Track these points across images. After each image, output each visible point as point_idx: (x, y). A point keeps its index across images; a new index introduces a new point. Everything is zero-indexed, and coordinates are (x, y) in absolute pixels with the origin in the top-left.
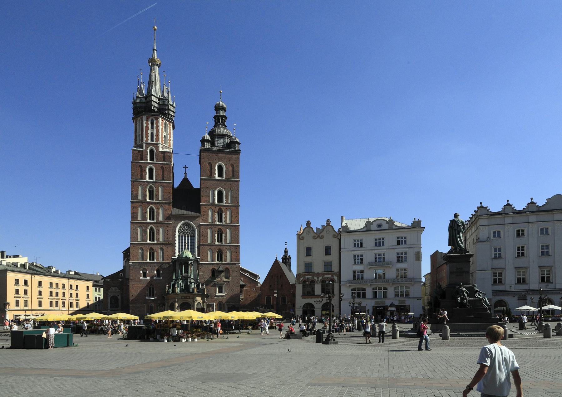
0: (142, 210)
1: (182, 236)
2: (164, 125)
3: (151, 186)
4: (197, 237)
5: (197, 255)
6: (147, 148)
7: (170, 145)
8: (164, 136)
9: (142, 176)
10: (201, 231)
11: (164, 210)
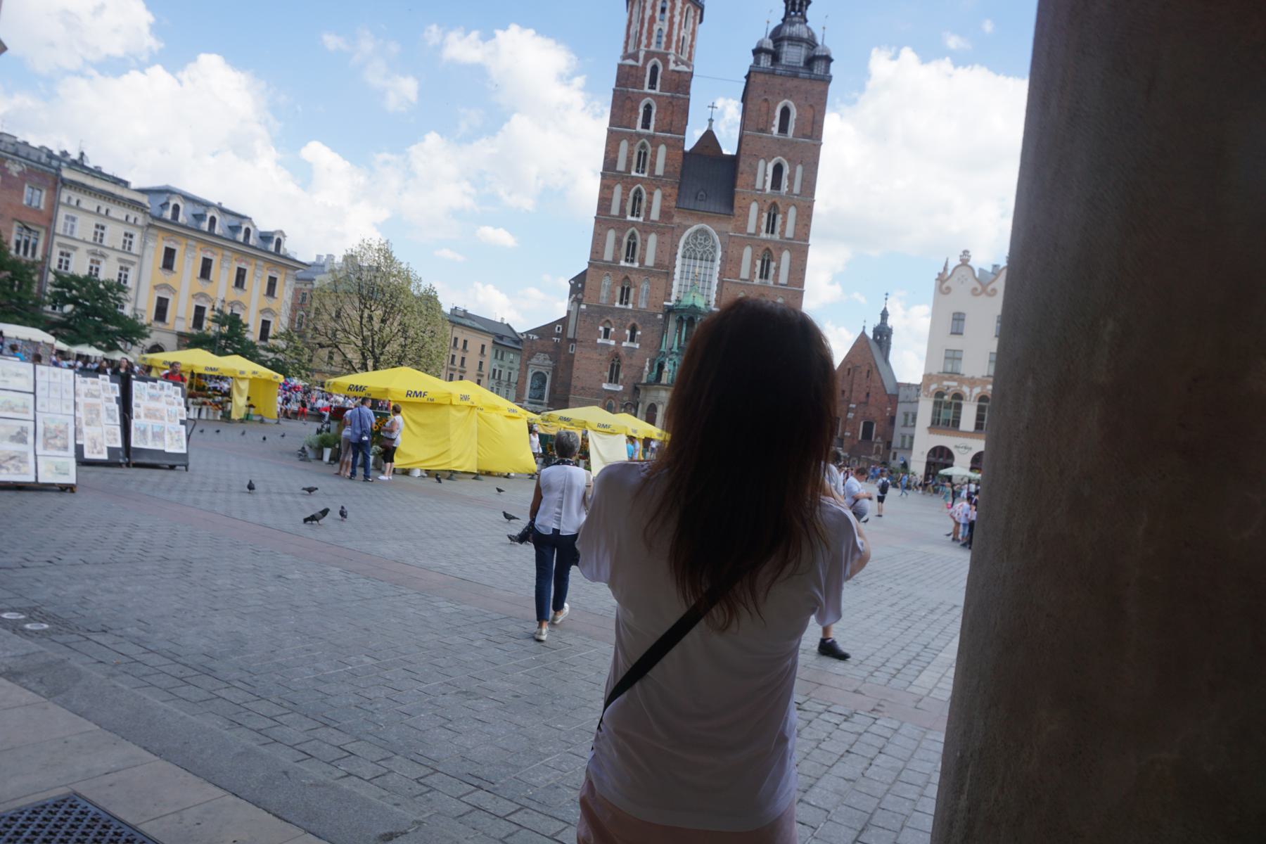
0: (623, 194)
3: (644, 143)
4: (718, 262)
8: (681, 38)
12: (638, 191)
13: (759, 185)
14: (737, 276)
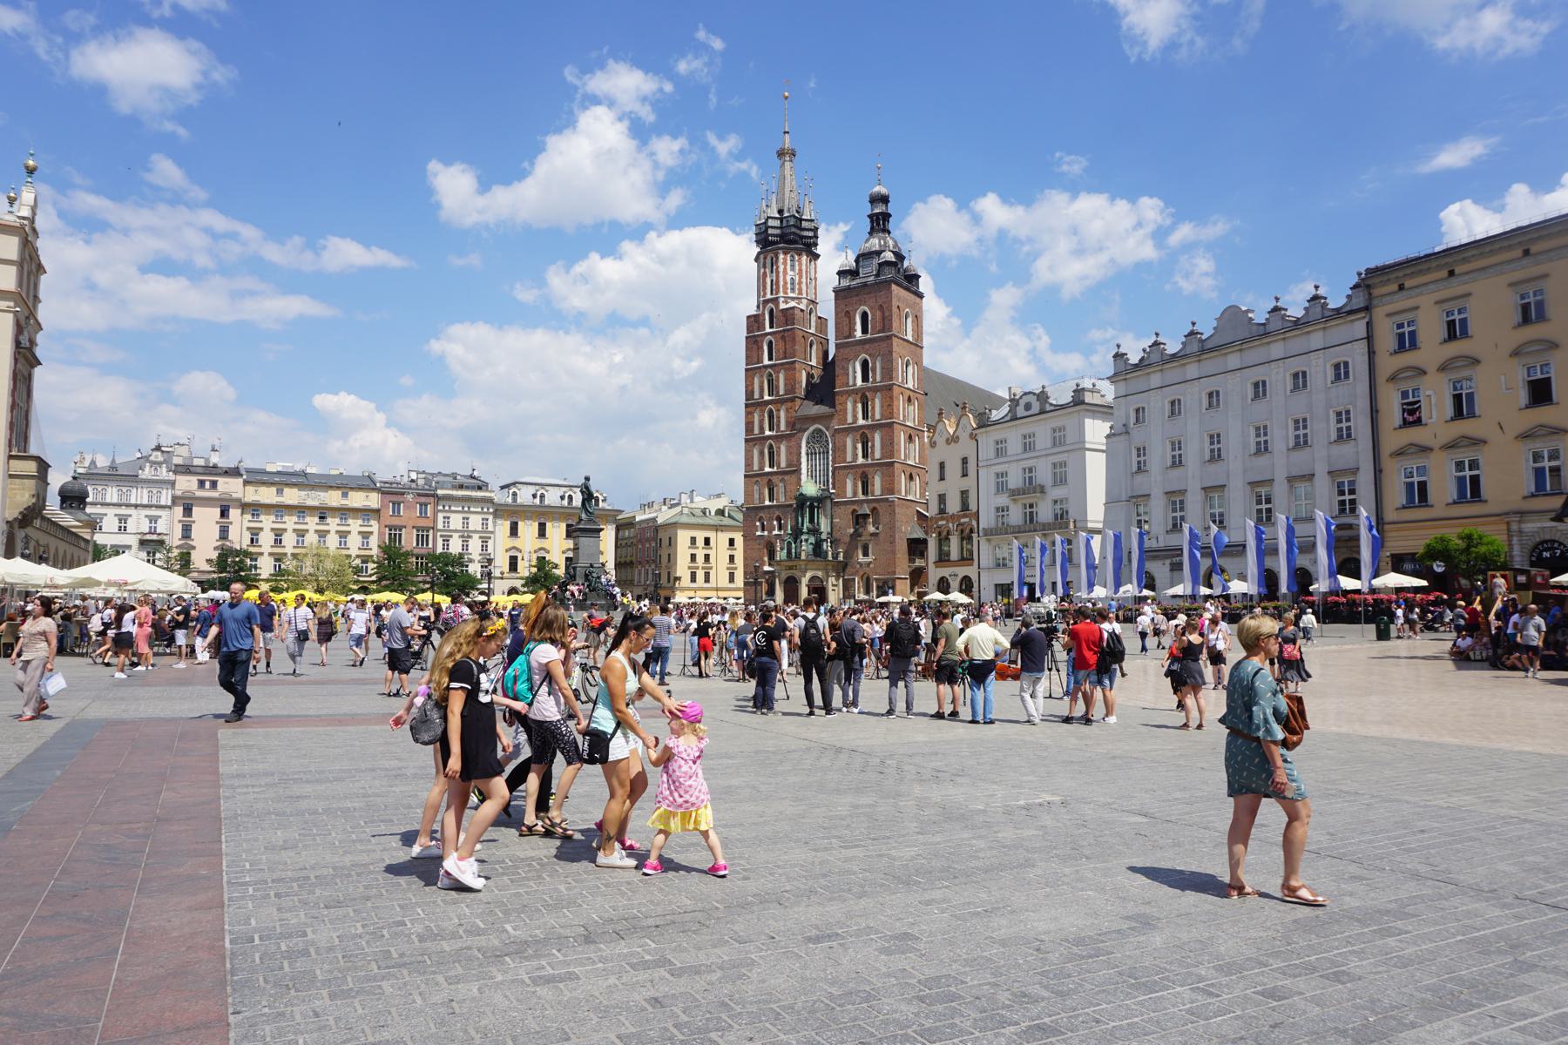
2: (789, 262)
5: (831, 486)
6: (764, 308)
7: (800, 293)
9: (760, 360)
11: (787, 410)
12: (771, 412)
13: (851, 383)
14: (845, 461)
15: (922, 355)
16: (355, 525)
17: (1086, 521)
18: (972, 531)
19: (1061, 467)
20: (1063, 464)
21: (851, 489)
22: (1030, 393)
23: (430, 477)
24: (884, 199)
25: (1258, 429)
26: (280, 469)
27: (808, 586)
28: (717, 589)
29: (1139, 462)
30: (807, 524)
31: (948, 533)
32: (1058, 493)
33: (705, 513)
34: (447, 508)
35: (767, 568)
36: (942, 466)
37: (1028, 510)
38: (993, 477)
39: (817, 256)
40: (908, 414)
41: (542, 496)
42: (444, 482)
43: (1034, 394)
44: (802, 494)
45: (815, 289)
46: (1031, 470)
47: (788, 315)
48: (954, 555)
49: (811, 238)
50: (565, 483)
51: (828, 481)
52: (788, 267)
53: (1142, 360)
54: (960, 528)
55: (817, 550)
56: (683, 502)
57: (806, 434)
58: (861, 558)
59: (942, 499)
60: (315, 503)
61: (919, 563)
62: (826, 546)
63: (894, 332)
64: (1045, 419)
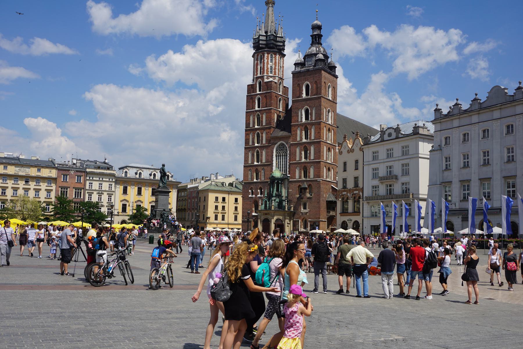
0: (253, 136)
1: (278, 156)
2: (270, 58)
3: (258, 114)
4: (288, 155)
5: (288, 173)
6: (256, 81)
7: (275, 74)
10: (291, 150)
11: (267, 134)
12: (258, 134)
13: (299, 120)
14: (295, 160)
15: (336, 107)
16: (43, 186)
17: (419, 194)
18: (359, 198)
19: (406, 166)
20: (407, 165)
21: (298, 174)
22: (391, 128)
23: (83, 162)
24: (319, 28)
25: (508, 149)
26: (6, 156)
27: (274, 223)
28: (228, 224)
29: (446, 165)
30: (275, 192)
31: (348, 198)
32: (404, 179)
33: (223, 185)
34: (91, 178)
35: (254, 214)
36: (345, 164)
37: (389, 188)
38: (371, 170)
39: (285, 55)
40: (328, 137)
41: (140, 174)
42: (90, 165)
43: (393, 128)
44: (273, 176)
45: (283, 72)
46: (390, 167)
47: (269, 85)
48: (350, 210)
49: (281, 46)
50: (152, 167)
51: (286, 170)
52: (269, 61)
53: (449, 112)
54: (354, 196)
55: (280, 205)
56: (212, 179)
57: (276, 146)
58: (302, 210)
59: (345, 181)
60: (24, 174)
61: (332, 213)
62: (285, 203)
63: (322, 95)
64: (398, 141)
